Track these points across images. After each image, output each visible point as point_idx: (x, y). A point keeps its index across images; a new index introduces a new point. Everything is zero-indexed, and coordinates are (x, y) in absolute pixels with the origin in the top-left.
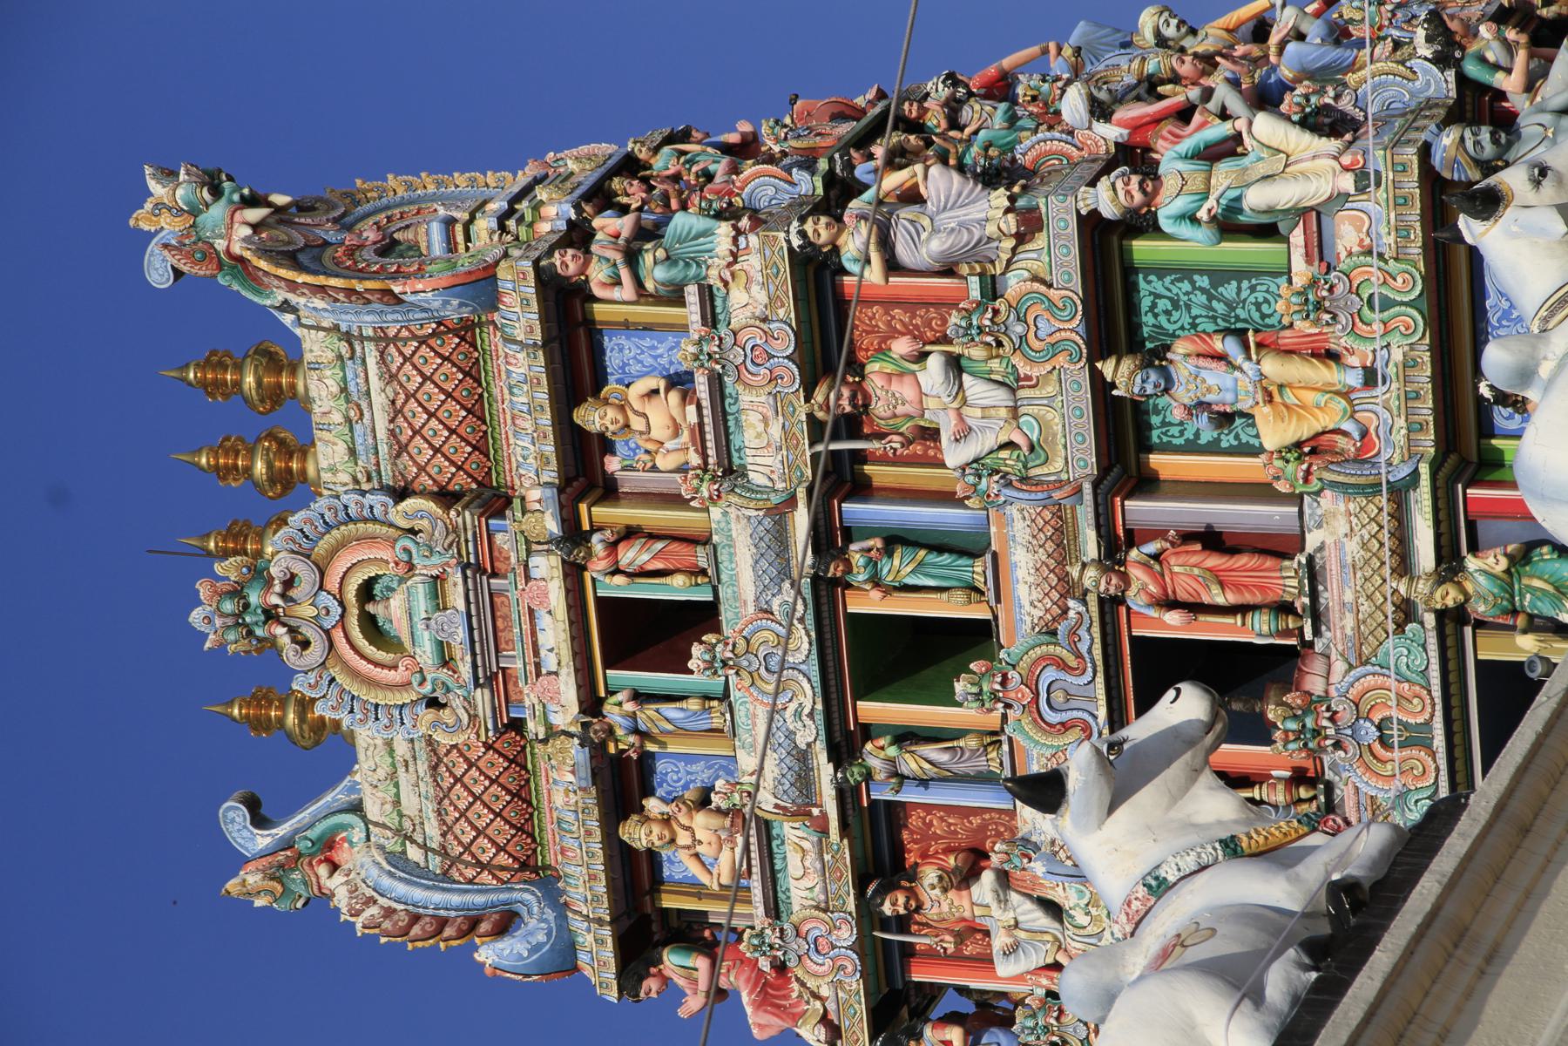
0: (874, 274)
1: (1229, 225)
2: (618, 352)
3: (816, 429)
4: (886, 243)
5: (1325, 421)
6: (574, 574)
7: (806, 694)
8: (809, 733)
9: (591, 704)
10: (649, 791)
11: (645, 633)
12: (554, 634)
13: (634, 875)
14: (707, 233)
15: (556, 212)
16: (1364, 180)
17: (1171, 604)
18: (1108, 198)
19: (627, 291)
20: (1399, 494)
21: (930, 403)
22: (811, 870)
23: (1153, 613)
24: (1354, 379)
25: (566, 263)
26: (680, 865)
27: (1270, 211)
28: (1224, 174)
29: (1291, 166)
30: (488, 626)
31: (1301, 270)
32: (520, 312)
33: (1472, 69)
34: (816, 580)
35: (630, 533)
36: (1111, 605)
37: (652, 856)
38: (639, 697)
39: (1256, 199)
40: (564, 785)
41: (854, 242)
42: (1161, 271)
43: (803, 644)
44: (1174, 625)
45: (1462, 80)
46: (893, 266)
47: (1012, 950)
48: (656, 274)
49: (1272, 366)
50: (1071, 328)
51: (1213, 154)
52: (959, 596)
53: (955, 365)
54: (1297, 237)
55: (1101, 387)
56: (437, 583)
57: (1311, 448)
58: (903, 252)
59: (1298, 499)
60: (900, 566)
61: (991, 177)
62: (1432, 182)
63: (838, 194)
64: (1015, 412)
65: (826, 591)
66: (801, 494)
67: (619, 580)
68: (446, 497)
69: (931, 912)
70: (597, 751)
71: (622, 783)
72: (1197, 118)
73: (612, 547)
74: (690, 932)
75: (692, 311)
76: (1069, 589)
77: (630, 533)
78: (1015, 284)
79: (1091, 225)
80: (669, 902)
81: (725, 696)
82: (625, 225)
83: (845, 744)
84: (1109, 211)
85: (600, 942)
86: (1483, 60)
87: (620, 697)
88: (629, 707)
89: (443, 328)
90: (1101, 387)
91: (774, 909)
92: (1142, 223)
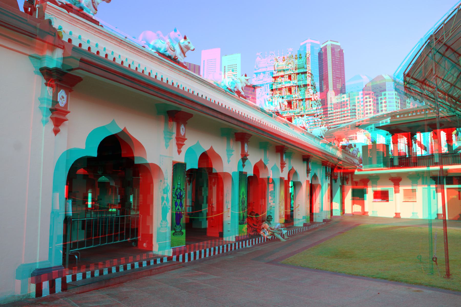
1: (311, 105)
11: (290, 77)
12: (289, 73)
13: (278, 77)
15: (310, 72)
18: (313, 99)
22: (279, 86)
26: (278, 79)
32: (305, 71)
40: (282, 73)
41: (310, 87)
61: (313, 93)
63: (312, 86)
65: (293, 86)
71: (282, 76)
74: (275, 80)
79: (311, 98)
83: (285, 87)
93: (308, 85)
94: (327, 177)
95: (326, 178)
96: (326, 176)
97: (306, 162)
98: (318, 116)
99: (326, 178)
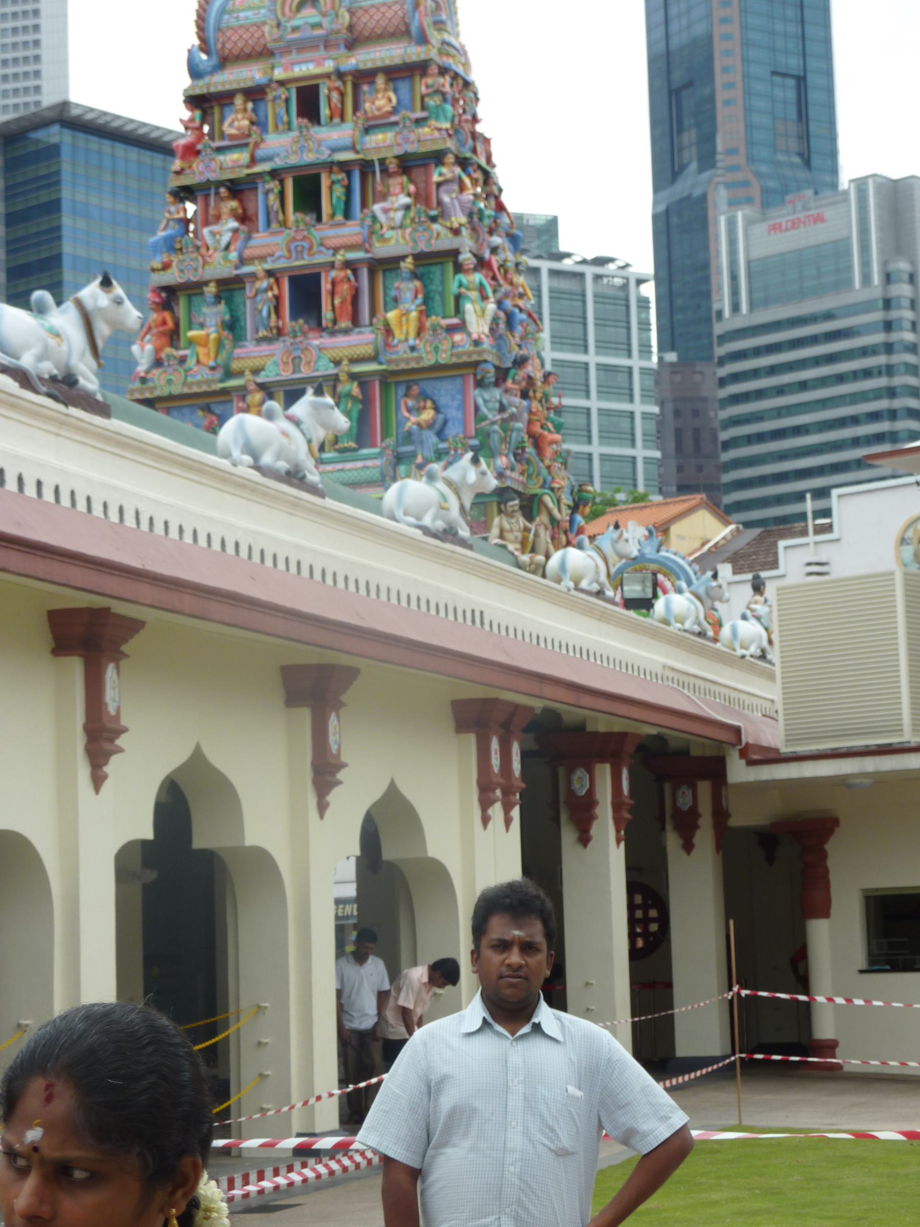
0: (436, 178)
2: (404, 86)
3: (382, 161)
4: (447, 182)
5: (397, 333)
6: (328, 76)
7: (293, 160)
8: (278, 163)
9: (281, 83)
10: (254, 101)
14: (446, 117)
16: (477, 343)
17: (334, 283)
18: (466, 257)
19: (424, 89)
20: (374, 358)
21: (394, 199)
23: (330, 280)
24: (411, 342)
25: (434, 69)
27: (464, 313)
28: (474, 294)
29: (478, 319)
30: (305, 46)
31: (445, 322)
33: (513, 372)
34: (332, 163)
35: (342, 95)
36: (332, 265)
37: (232, 104)
38: (287, 100)
39: (468, 307)
42: (443, 275)
43: (309, 158)
44: (325, 287)
45: (508, 370)
46: (439, 185)
47: (213, 234)
48: (431, 102)
49: (414, 314)
50: (423, 247)
51: (481, 289)
52: (330, 212)
53: (407, 208)
54: (455, 321)
55: (403, 258)
56: (319, 25)
57: (388, 331)
58: (443, 189)
59: (371, 324)
60: (339, 191)
62: (476, 364)
64: (393, 228)
65: (330, 166)
66: (360, 156)
67: (326, 91)
68: (351, 28)
69: (222, 205)
70: (268, 85)
71: (255, 94)
72: (493, 283)
73: (337, 89)
75: (419, 114)
76: (336, 250)
77: (342, 95)
78: (436, 227)
79: (455, 253)
80: (217, 111)
81: (290, 129)
82: (447, 88)
83: (275, 174)
84: (461, 257)
85: (201, 88)
86: (515, 375)
87: (287, 93)
88: (283, 97)
89: (407, 26)
90: (403, 258)
91: (219, 150)
92: (459, 268)
93: (438, 157)
94: (496, 811)
95: (485, 820)
96: (485, 804)
97: (304, 716)
98: (502, 375)
99: (485, 820)
